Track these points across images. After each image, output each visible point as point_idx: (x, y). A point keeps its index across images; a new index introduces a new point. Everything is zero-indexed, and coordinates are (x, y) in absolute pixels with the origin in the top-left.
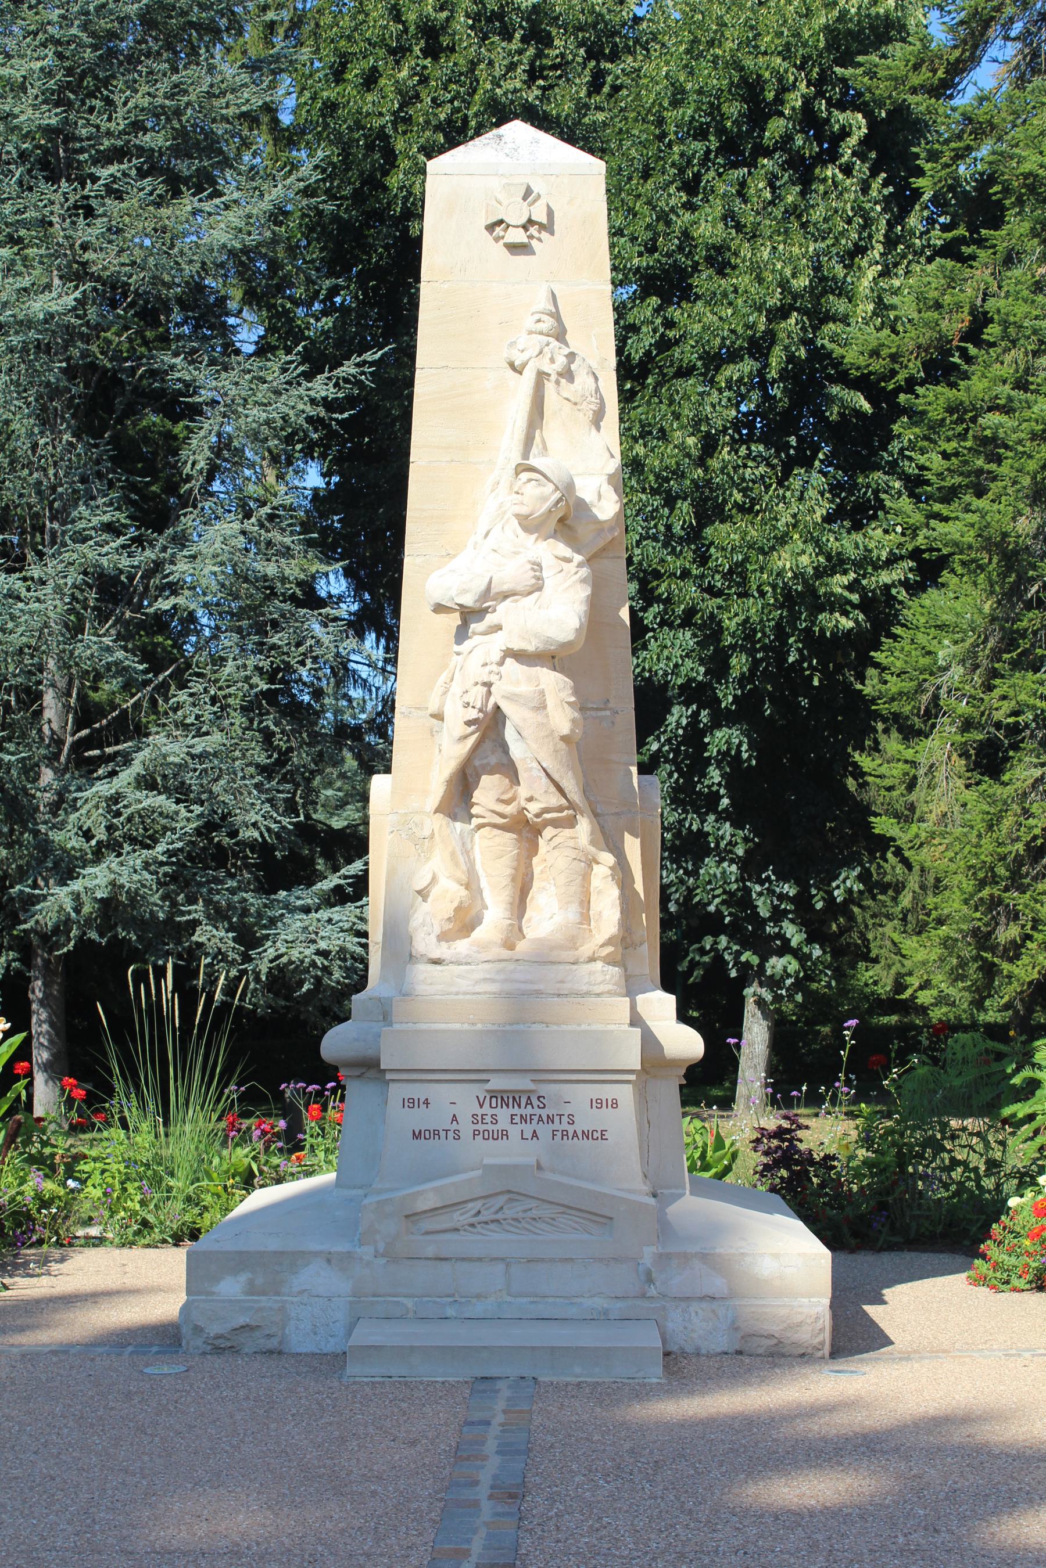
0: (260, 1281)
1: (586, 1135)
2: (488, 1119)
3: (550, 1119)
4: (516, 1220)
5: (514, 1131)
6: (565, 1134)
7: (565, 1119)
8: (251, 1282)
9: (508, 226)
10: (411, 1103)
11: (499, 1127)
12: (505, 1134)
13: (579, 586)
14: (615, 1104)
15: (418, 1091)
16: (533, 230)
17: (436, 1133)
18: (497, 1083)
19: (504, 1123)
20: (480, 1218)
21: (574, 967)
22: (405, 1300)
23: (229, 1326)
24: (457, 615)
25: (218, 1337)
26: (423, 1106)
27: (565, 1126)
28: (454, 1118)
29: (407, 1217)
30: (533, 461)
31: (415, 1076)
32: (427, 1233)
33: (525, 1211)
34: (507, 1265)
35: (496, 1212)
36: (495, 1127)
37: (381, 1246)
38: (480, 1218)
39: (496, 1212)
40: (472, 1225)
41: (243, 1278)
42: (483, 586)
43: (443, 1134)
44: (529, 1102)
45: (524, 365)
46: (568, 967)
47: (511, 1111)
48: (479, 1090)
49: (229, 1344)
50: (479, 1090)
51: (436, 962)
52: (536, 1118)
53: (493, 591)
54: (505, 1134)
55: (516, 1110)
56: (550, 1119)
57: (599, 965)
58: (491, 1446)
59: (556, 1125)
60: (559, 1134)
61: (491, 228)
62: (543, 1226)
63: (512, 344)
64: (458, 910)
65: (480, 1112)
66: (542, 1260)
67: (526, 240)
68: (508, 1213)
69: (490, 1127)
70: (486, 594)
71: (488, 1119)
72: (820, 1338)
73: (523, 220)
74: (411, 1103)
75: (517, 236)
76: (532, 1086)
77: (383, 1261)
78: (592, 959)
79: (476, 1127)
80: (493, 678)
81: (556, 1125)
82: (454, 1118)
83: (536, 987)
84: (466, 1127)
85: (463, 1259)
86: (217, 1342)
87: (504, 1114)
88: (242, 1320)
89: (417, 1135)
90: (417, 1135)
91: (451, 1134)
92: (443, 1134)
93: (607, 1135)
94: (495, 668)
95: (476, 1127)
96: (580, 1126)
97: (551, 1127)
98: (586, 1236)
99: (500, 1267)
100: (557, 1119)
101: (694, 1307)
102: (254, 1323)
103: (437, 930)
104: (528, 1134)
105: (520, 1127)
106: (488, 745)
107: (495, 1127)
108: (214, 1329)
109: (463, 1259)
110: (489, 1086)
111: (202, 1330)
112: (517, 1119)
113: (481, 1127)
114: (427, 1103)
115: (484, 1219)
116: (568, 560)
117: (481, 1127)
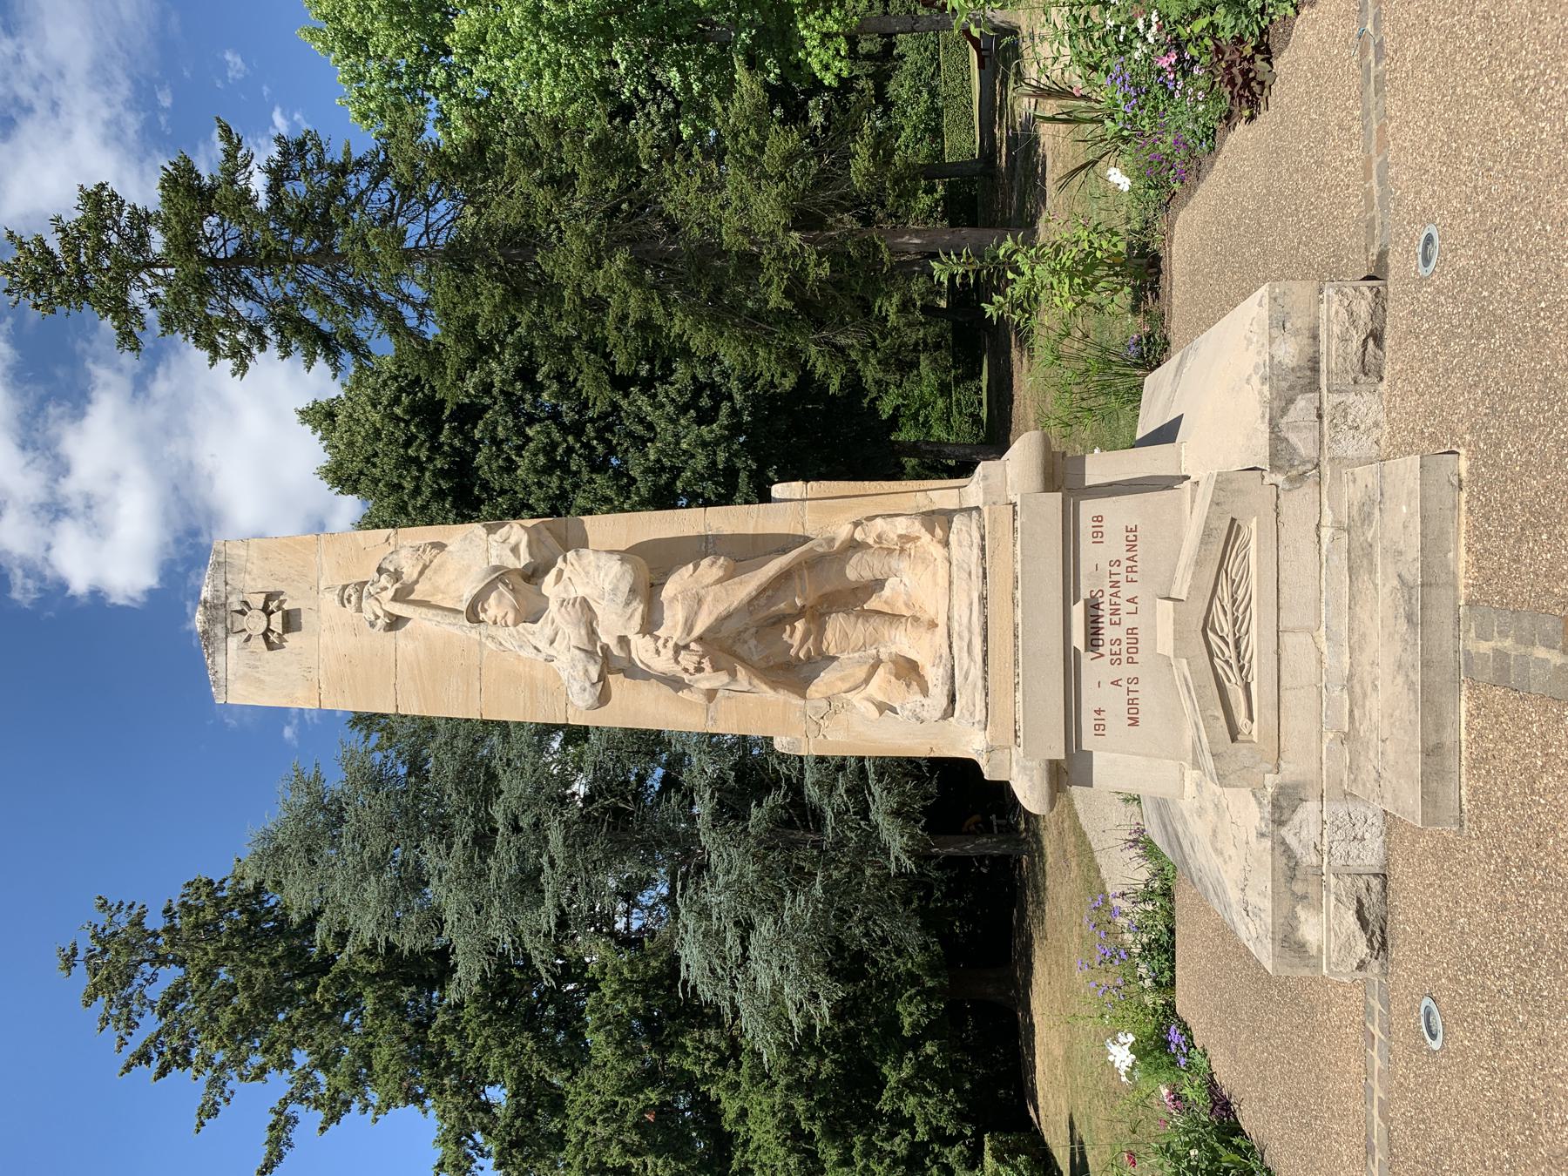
1: (1131, 547)
2: (1115, 648)
3: (1115, 584)
4: (1235, 620)
5: (1128, 622)
6: (1130, 570)
7: (1115, 569)
9: (268, 629)
12: (1131, 631)
13: (585, 561)
14: (1098, 519)
16: (273, 605)
17: (1131, 702)
18: (1078, 640)
19: (1120, 632)
20: (1233, 661)
21: (954, 562)
22: (1326, 741)
23: (1358, 932)
24: (611, 678)
29: (1234, 739)
30: (463, 607)
32: (1251, 719)
33: (1225, 613)
35: (1227, 644)
38: (1233, 661)
39: (1227, 644)
40: (1241, 669)
42: (582, 655)
43: (1132, 695)
45: (388, 614)
46: (954, 568)
49: (1378, 932)
50: (1086, 658)
52: (1114, 600)
53: (589, 648)
56: (1115, 584)
57: (953, 538)
58: (1485, 647)
59: (1122, 578)
60: (1131, 575)
61: (270, 646)
62: (1241, 592)
63: (372, 625)
64: (898, 677)
65: (1108, 657)
68: (1227, 629)
69: (1124, 646)
70: (590, 654)
71: (1115, 648)
72: (1367, 292)
73: (262, 614)
74: (1099, 727)
75: (277, 619)
76: (1081, 604)
78: (946, 544)
79: (1124, 661)
80: (671, 644)
81: (1122, 578)
83: (976, 601)
84: (1125, 671)
86: (1377, 946)
87: (1108, 633)
88: (1351, 918)
89: (1134, 722)
90: (1134, 722)
91: (1132, 687)
92: (1132, 695)
94: (661, 642)
95: (1124, 661)
96: (1123, 554)
97: (1123, 585)
98: (1253, 545)
99: (1287, 639)
100: (1114, 578)
102: (1354, 906)
103: (919, 697)
104: (1132, 607)
105: (1124, 617)
106: (738, 648)
108: (1362, 949)
110: (1081, 648)
111: (1363, 961)
112: (1115, 619)
113: (1124, 656)
114: (1099, 712)
115: (1234, 655)
116: (561, 572)
117: (1124, 656)
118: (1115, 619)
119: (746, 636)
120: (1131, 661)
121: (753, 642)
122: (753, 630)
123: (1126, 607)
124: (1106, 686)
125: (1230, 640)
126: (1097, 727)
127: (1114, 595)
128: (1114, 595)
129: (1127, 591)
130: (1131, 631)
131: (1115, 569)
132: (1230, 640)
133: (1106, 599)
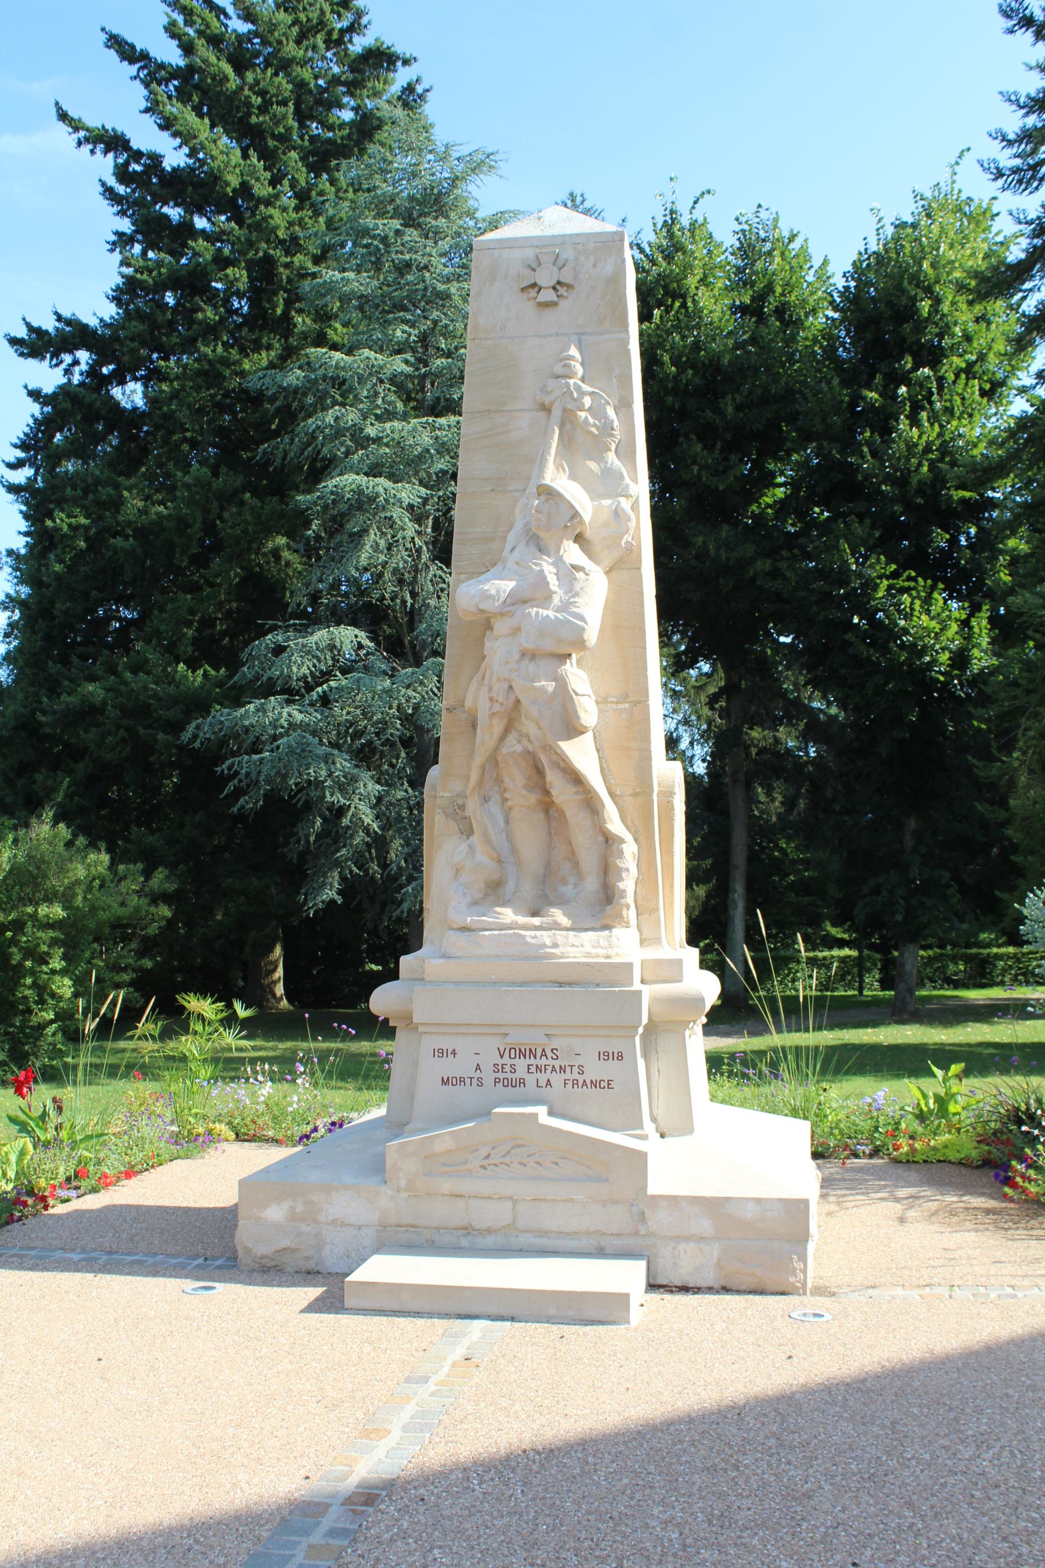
0: (300, 1209)
5: (531, 1080)
6: (575, 1082)
7: (575, 1070)
8: (292, 1209)
10: (440, 1053)
11: (517, 1075)
15: (447, 1044)
17: (462, 1080)
25: (262, 1257)
26: (451, 1056)
27: (575, 1076)
28: (478, 1067)
31: (443, 1029)
33: (530, 1156)
34: (515, 1202)
36: (514, 1076)
37: (403, 1183)
41: (286, 1205)
43: (468, 1081)
44: (544, 1054)
45: (552, 404)
47: (528, 1061)
48: (498, 1043)
51: (465, 929)
52: (550, 1068)
54: (522, 1082)
55: (532, 1061)
59: (568, 1075)
60: (570, 1083)
65: (500, 1062)
66: (546, 1200)
67: (555, 299)
69: (509, 1076)
71: (507, 1068)
73: (553, 282)
74: (440, 1053)
75: (547, 295)
77: (405, 1195)
81: (568, 1075)
82: (478, 1067)
84: (488, 1076)
85: (475, 1197)
86: (263, 1261)
87: (521, 1064)
88: (285, 1243)
89: (445, 1082)
90: (445, 1082)
91: (474, 1081)
92: (468, 1081)
93: (613, 1084)
97: (563, 1076)
99: (509, 1204)
100: (568, 1069)
101: (682, 1247)
107: (514, 1076)
109: (475, 1197)
112: (533, 1069)
113: (501, 1075)
114: (454, 1053)
117: (501, 1075)
118: (533, 1069)
119: (525, 742)
120: (496, 1081)
121: (519, 748)
122: (531, 748)
123: (543, 1078)
124: (477, 1060)
125: (507, 1160)
126: (441, 1051)
127: (554, 1069)
128: (554, 1069)
129: (557, 1079)
130: (522, 1082)
131: (575, 1070)
132: (507, 1160)
133: (551, 1062)
